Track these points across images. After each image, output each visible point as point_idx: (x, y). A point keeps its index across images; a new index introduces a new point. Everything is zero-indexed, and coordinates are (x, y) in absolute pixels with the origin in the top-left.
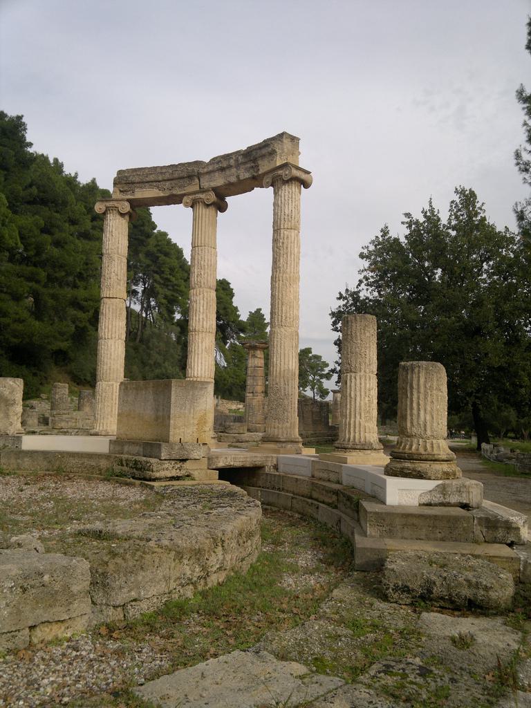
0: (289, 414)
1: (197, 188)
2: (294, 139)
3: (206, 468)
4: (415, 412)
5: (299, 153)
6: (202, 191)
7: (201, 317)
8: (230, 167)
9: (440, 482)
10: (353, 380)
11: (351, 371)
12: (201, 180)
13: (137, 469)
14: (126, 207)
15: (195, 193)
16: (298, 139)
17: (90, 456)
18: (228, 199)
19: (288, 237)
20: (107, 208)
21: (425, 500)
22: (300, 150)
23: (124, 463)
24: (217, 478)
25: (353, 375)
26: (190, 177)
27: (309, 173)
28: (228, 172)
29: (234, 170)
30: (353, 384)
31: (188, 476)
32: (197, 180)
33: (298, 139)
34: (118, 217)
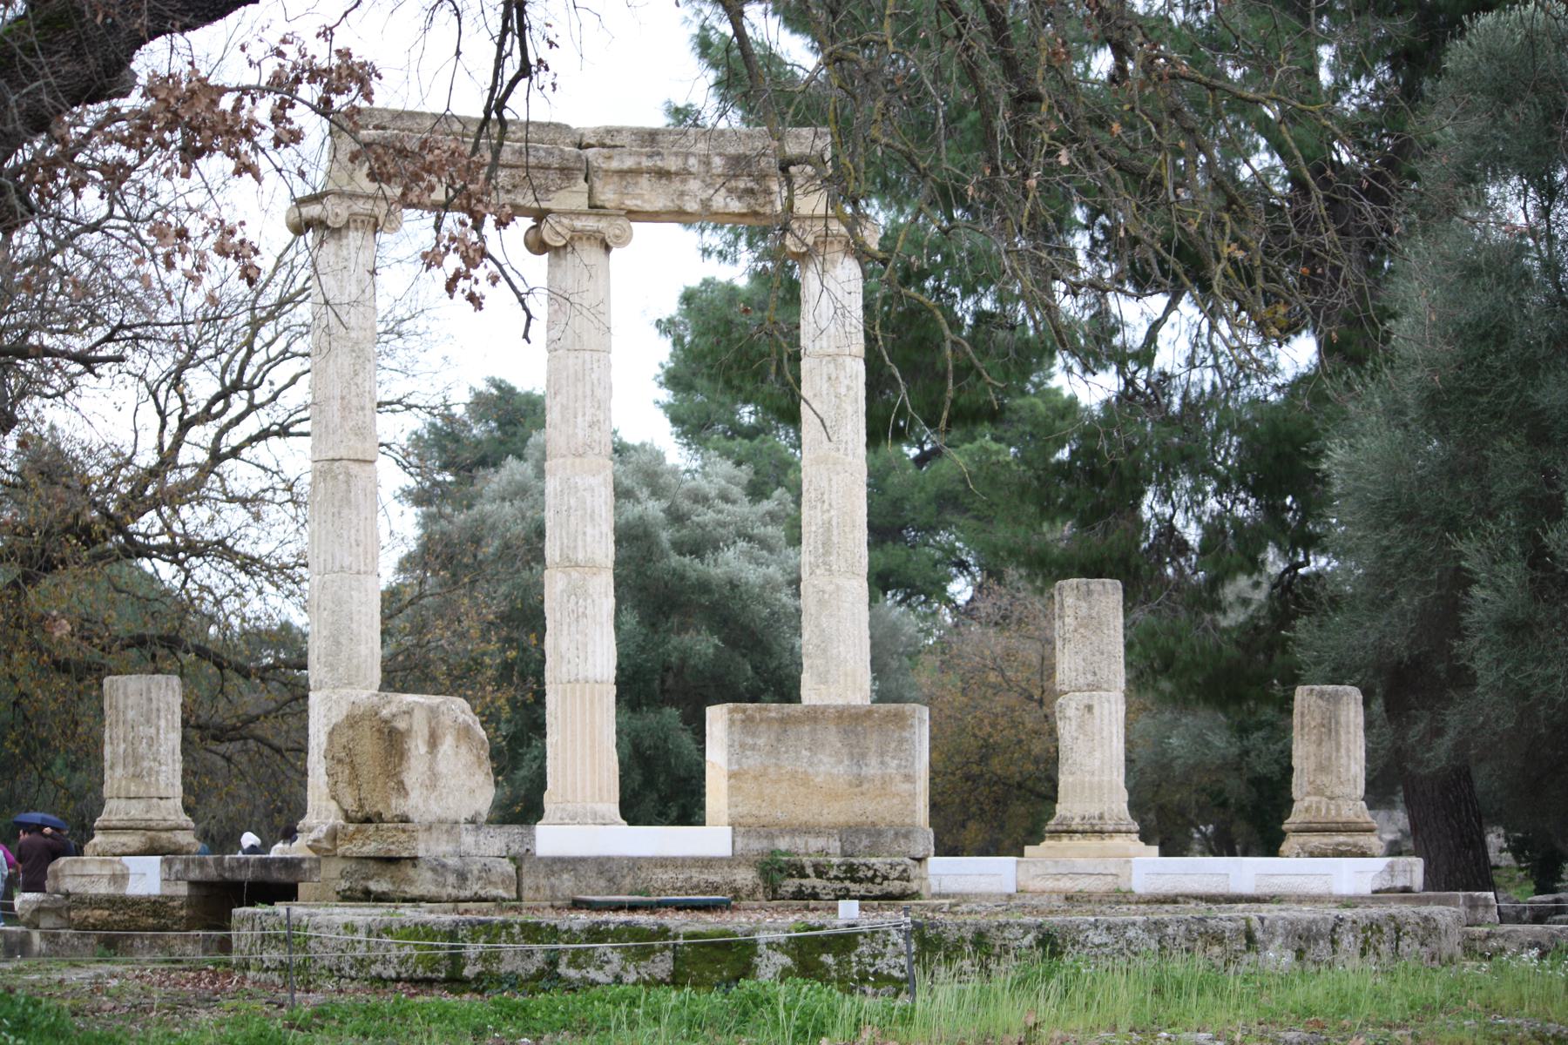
1: (582, 202)
4: (1343, 761)
8: (685, 173)
10: (1106, 705)
11: (1099, 688)
12: (598, 184)
13: (853, 880)
15: (579, 214)
17: (707, 863)
21: (1376, 887)
23: (809, 871)
25: (1103, 693)
26: (566, 172)
28: (676, 184)
29: (694, 185)
30: (1106, 712)
32: (582, 185)
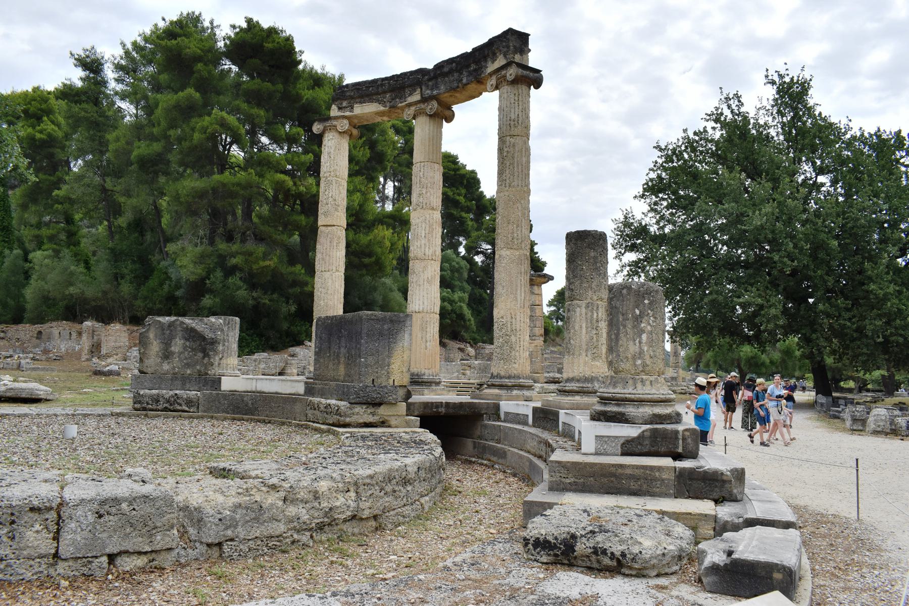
0: (517, 354)
2: (523, 38)
3: (405, 413)
5: (530, 50)
6: (424, 100)
7: (423, 242)
9: (648, 426)
14: (344, 125)
16: (528, 35)
18: (455, 108)
19: (514, 146)
20: (325, 127)
22: (530, 47)
24: (418, 423)
27: (538, 71)
31: (383, 422)
33: (528, 35)
34: (336, 135)
